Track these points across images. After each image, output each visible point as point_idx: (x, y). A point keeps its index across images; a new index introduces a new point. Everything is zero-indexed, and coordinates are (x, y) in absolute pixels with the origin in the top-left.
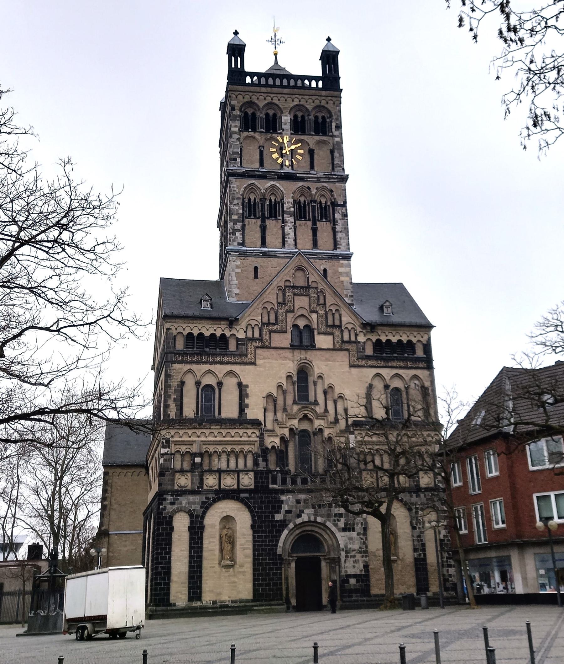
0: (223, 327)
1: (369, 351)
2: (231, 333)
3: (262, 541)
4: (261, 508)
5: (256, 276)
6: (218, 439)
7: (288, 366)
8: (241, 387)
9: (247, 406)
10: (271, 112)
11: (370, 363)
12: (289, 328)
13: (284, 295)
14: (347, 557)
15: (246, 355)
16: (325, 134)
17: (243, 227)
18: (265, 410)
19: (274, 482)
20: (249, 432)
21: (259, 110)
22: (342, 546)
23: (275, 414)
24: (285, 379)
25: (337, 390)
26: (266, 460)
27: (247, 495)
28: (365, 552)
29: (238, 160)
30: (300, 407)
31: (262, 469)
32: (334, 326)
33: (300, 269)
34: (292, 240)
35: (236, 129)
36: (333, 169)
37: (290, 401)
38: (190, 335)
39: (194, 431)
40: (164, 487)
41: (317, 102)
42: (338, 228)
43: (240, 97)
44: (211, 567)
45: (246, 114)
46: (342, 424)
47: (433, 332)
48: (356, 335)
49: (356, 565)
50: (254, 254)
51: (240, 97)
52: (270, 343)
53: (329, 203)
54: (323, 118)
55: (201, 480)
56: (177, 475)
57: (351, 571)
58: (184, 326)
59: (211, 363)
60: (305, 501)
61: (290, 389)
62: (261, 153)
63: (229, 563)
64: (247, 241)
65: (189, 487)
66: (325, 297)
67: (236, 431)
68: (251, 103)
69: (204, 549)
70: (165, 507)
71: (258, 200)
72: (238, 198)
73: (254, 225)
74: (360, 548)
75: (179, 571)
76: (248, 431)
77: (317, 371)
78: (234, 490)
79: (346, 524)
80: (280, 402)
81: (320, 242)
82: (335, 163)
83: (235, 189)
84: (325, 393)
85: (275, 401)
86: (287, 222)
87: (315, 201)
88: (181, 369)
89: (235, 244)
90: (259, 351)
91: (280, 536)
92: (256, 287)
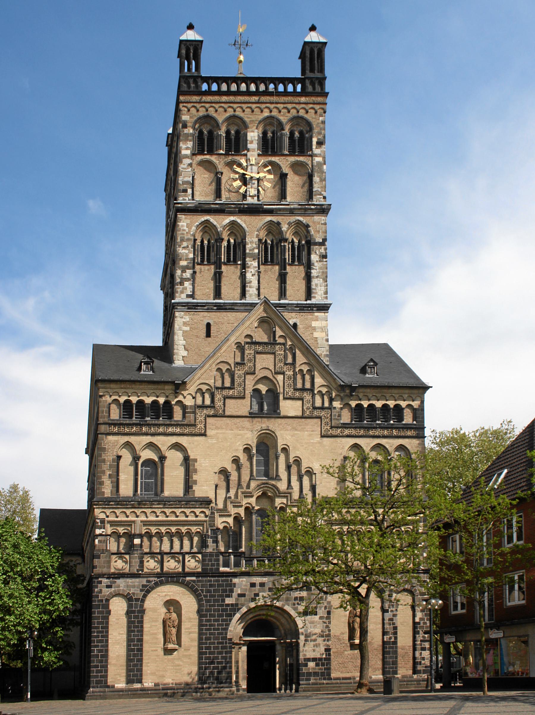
1: (346, 417)
2: (177, 399)
3: (210, 625)
4: (208, 591)
6: (160, 518)
7: (246, 436)
8: (187, 462)
9: (195, 482)
11: (347, 432)
14: (306, 640)
15: (195, 425)
16: (302, 153)
18: (216, 486)
19: (226, 564)
21: (218, 125)
24: (242, 451)
25: (304, 465)
26: (216, 542)
27: (194, 578)
28: (326, 636)
29: (190, 191)
30: (259, 482)
31: (211, 550)
32: (303, 389)
35: (188, 152)
37: (246, 477)
44: (152, 651)
49: (317, 649)
52: (224, 410)
55: (142, 562)
57: (310, 655)
59: (153, 435)
60: (262, 585)
67: (183, 510)
68: (207, 119)
69: (144, 633)
70: (101, 590)
72: (188, 240)
75: (117, 654)
76: (196, 510)
78: (179, 573)
80: (234, 477)
82: (314, 190)
83: (185, 228)
84: (288, 467)
88: (117, 441)
90: (210, 420)
91: (231, 620)
92: (208, 346)
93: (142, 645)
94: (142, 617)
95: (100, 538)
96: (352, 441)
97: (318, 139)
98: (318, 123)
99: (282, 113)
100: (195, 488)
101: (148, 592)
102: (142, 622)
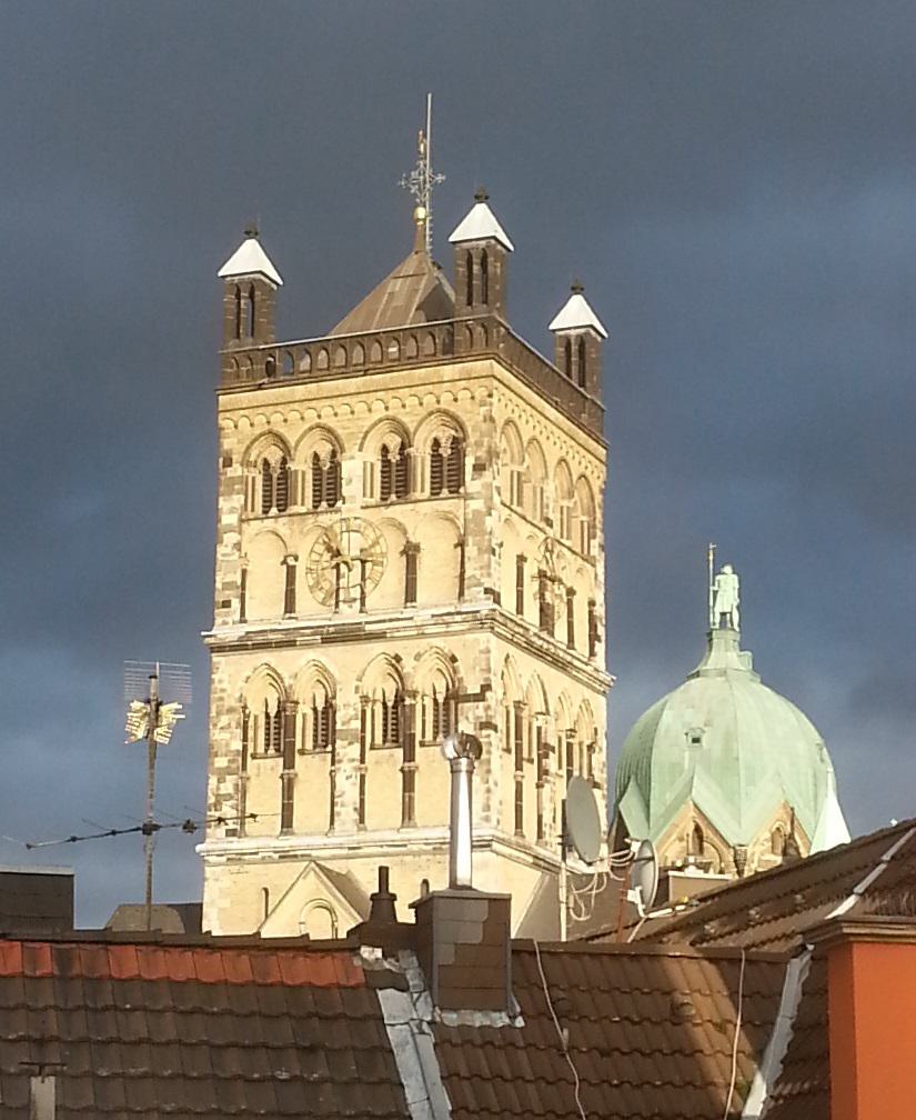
29: (236, 603)
34: (351, 809)
41: (429, 400)
50: (260, 855)
72: (231, 710)
83: (224, 686)
86: (340, 761)
97: (477, 458)
98: (477, 422)
99: (408, 409)
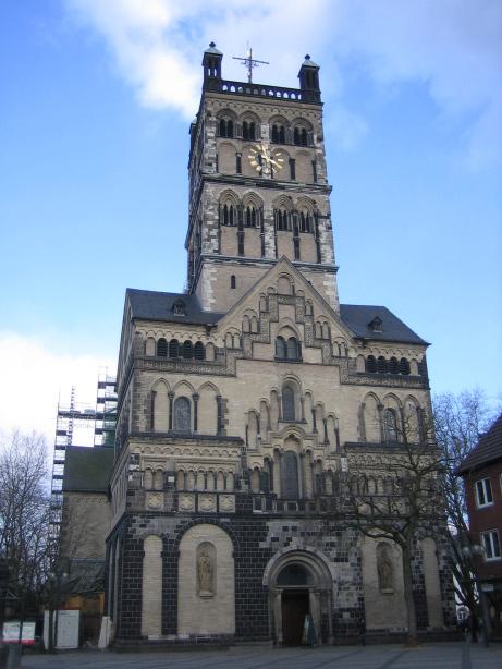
0: (200, 334)
1: (361, 368)
4: (243, 534)
5: (233, 286)
8: (220, 402)
9: (227, 422)
10: (249, 122)
11: (362, 381)
12: (273, 338)
13: (267, 303)
14: (340, 589)
16: (304, 144)
17: (219, 233)
18: (247, 427)
19: (258, 508)
20: (230, 450)
22: (334, 577)
23: (259, 432)
25: (327, 410)
26: (248, 483)
27: (228, 520)
28: (359, 584)
29: (214, 165)
32: (322, 339)
33: (285, 276)
35: (213, 135)
36: (315, 180)
37: (274, 420)
38: (162, 340)
39: (167, 446)
40: (133, 507)
41: (298, 114)
42: (322, 240)
43: (217, 104)
45: (222, 121)
46: (333, 446)
47: (429, 351)
48: (347, 350)
49: (351, 598)
51: (217, 104)
53: (311, 214)
54: (303, 130)
55: (176, 501)
56: (148, 494)
57: (345, 605)
58: (156, 330)
59: (187, 373)
60: (294, 529)
61: (275, 405)
62: (239, 160)
63: (207, 593)
64: (223, 249)
65: (162, 508)
66: (312, 308)
67: (216, 448)
71: (235, 207)
73: (230, 233)
74: (354, 579)
76: (228, 449)
77: (304, 388)
78: (212, 514)
79: (338, 554)
80: (264, 418)
81: (302, 255)
84: (313, 411)
85: (258, 418)
87: (297, 212)
89: (211, 251)
92: (234, 295)
93: (176, 591)
94: (177, 560)
95: (135, 474)
96: (368, 390)
100: (227, 427)
101: (183, 533)
102: (177, 566)
